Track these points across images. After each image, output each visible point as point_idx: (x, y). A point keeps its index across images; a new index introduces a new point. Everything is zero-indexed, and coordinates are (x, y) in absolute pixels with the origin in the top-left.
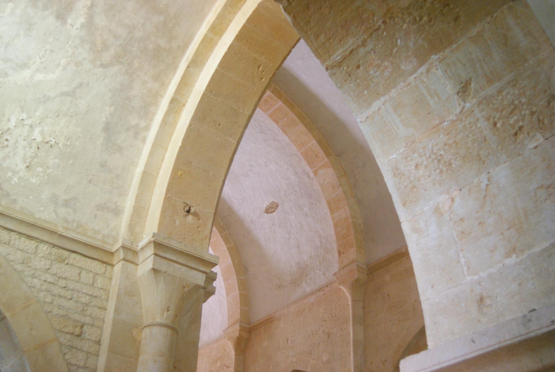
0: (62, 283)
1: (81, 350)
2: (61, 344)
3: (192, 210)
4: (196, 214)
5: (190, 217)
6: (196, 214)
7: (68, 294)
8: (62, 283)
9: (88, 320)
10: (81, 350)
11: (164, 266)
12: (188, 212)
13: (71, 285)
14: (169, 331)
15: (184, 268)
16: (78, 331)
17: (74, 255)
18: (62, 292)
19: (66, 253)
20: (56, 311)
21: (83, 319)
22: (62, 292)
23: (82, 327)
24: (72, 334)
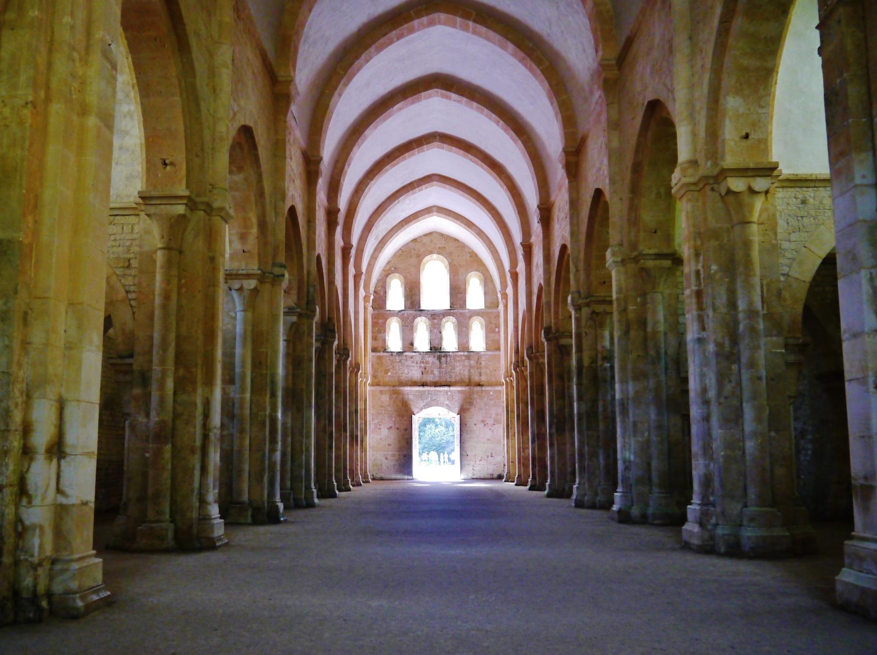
0: (112, 238)
1: (130, 275)
2: (118, 275)
3: (167, 162)
4: (172, 164)
5: (168, 168)
6: (172, 164)
7: (117, 243)
8: (112, 238)
9: (132, 256)
10: (130, 275)
11: (152, 210)
12: (165, 164)
13: (118, 237)
14: (166, 252)
15: (168, 206)
16: (126, 264)
17: (117, 217)
18: (114, 243)
19: (112, 218)
20: (112, 256)
21: (129, 256)
22: (114, 243)
23: (129, 260)
24: (123, 267)
